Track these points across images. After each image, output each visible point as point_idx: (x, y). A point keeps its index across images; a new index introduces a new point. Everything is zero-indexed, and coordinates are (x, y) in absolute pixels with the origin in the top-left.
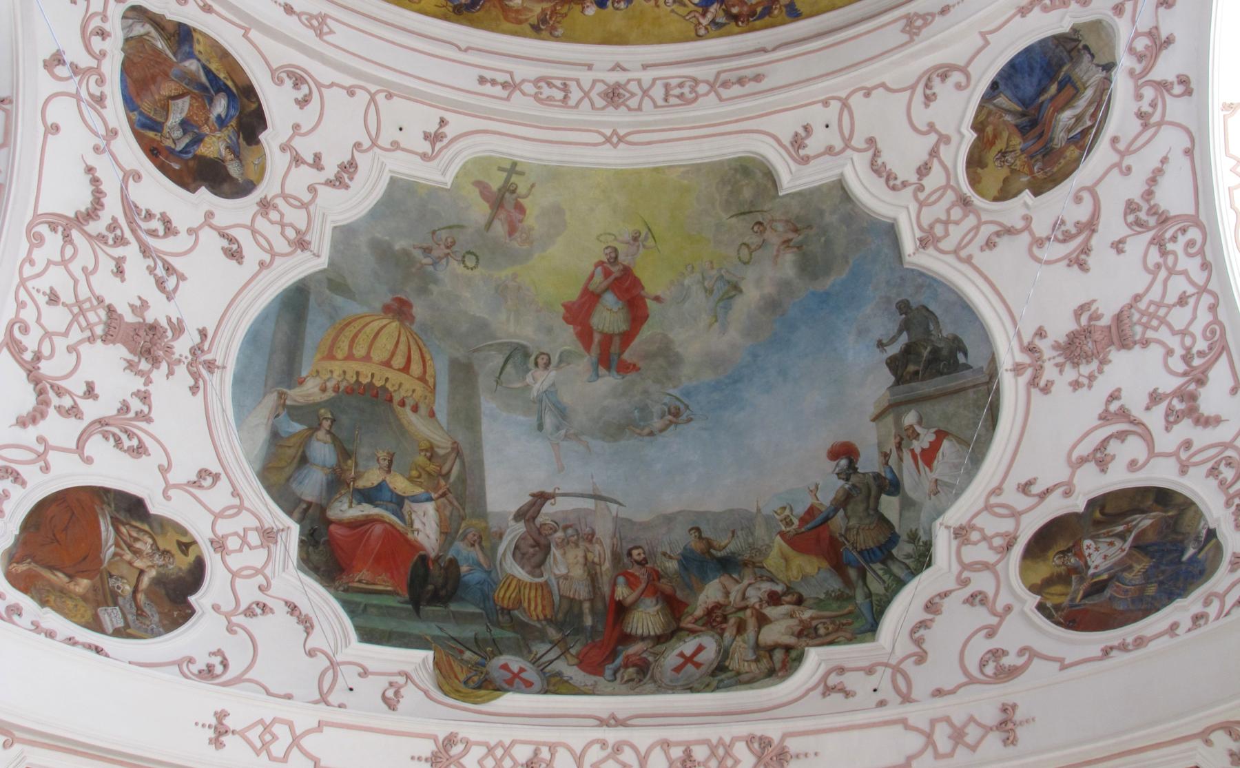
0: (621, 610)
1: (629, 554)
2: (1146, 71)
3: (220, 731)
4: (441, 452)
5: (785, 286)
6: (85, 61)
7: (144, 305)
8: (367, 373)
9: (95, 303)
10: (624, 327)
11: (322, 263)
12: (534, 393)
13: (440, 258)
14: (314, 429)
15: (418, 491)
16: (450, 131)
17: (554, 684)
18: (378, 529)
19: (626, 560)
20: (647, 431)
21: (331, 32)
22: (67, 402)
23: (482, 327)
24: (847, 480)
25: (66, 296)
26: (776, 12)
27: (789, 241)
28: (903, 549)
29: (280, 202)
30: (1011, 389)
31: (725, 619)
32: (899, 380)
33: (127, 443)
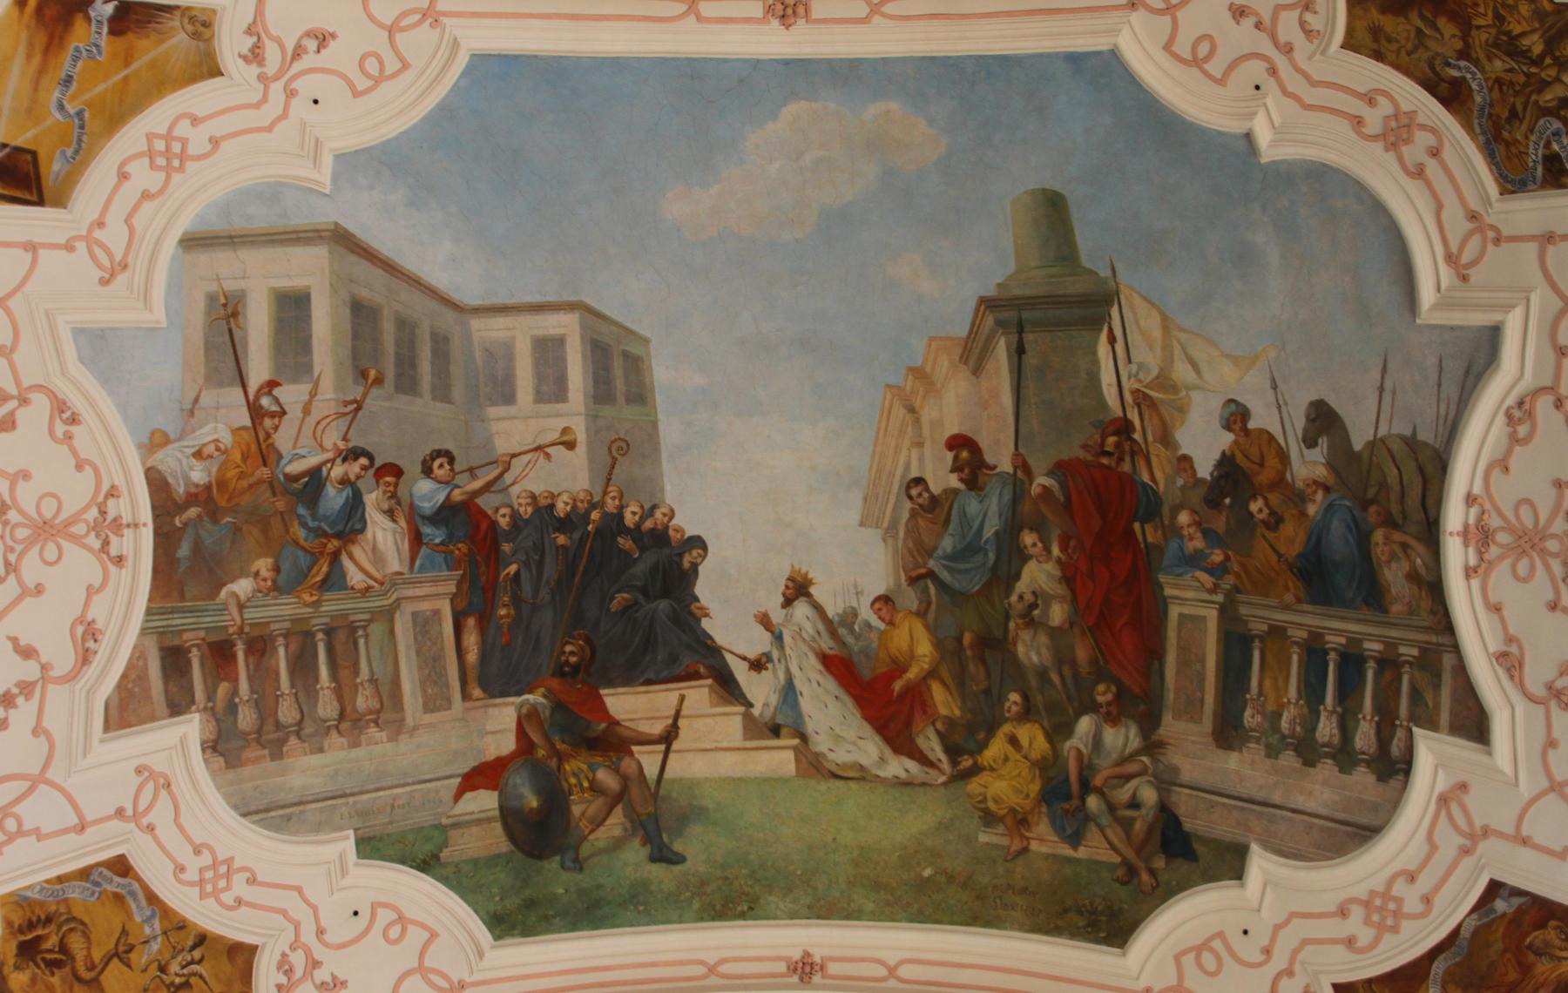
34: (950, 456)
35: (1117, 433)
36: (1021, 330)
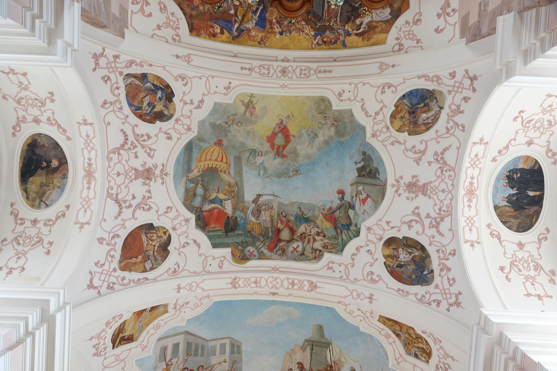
0: (279, 231)
1: (282, 214)
2: (453, 116)
3: (179, 289)
4: (232, 184)
5: (331, 137)
6: (114, 99)
7: (145, 163)
8: (210, 164)
9: (131, 169)
10: (283, 143)
11: (196, 134)
12: (258, 164)
13: (230, 125)
14: (197, 185)
15: (226, 197)
16: (232, 86)
17: (262, 257)
18: (216, 210)
19: (281, 215)
20: (288, 176)
21: (192, 60)
22: (128, 204)
23: (243, 144)
24: (341, 201)
25: (122, 171)
26: (338, 43)
27: (333, 124)
28: (353, 228)
29: (182, 118)
30: (390, 191)
31: (305, 238)
32: (359, 176)
33: (146, 208)
34: (297, 365)
35: (330, 367)
36: (313, 345)
